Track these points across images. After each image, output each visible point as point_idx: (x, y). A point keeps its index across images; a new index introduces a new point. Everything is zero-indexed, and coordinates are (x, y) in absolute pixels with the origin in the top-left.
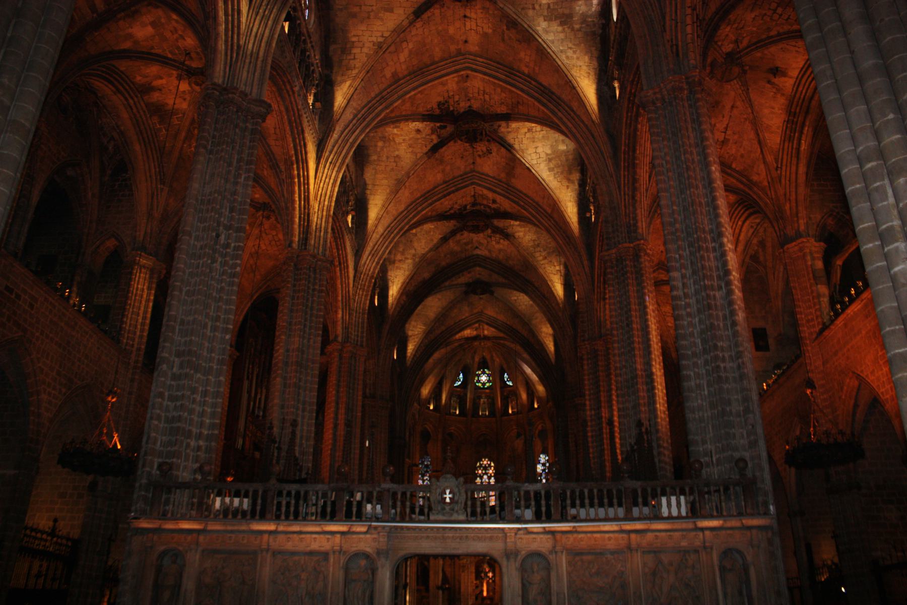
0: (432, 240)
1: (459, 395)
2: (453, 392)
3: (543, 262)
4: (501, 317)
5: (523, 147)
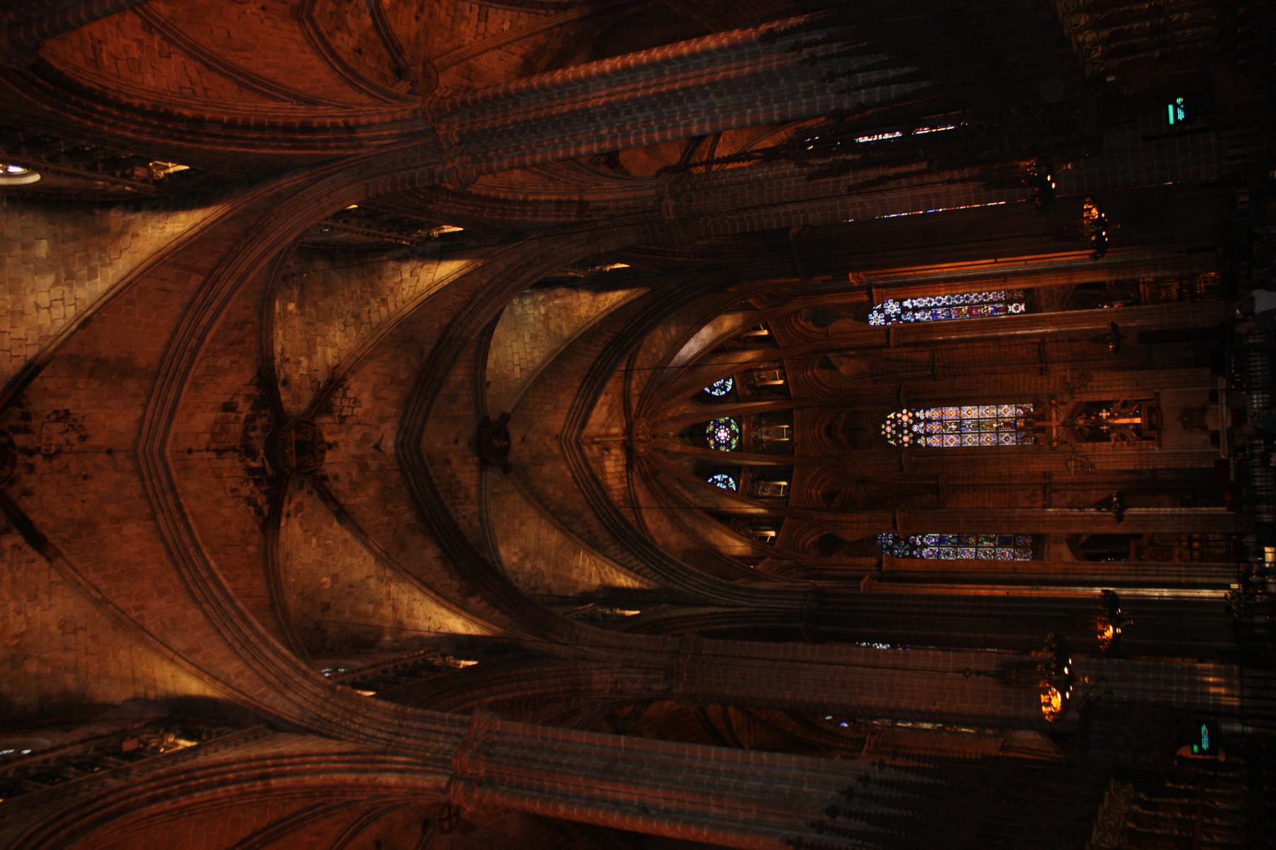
0: (345, 541)
1: (753, 480)
2: (749, 496)
3: (392, 308)
4: (567, 399)
5: (33, 336)
